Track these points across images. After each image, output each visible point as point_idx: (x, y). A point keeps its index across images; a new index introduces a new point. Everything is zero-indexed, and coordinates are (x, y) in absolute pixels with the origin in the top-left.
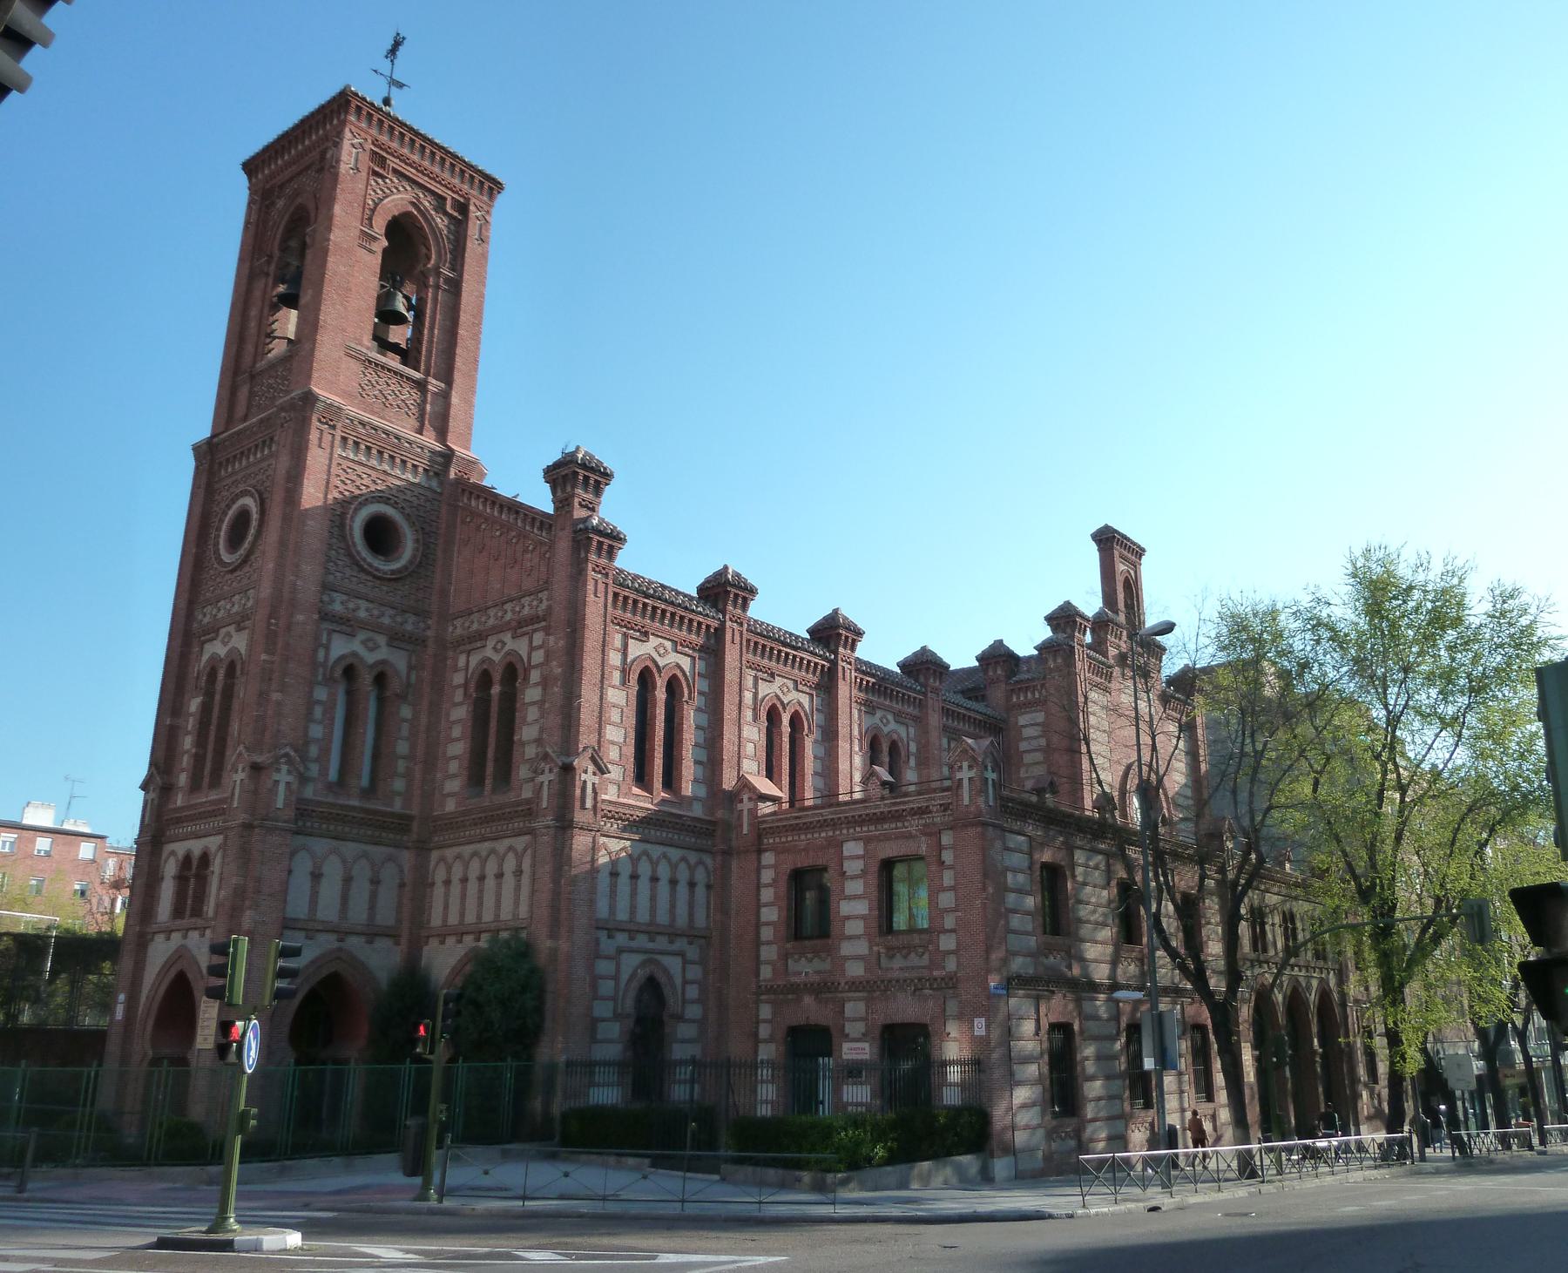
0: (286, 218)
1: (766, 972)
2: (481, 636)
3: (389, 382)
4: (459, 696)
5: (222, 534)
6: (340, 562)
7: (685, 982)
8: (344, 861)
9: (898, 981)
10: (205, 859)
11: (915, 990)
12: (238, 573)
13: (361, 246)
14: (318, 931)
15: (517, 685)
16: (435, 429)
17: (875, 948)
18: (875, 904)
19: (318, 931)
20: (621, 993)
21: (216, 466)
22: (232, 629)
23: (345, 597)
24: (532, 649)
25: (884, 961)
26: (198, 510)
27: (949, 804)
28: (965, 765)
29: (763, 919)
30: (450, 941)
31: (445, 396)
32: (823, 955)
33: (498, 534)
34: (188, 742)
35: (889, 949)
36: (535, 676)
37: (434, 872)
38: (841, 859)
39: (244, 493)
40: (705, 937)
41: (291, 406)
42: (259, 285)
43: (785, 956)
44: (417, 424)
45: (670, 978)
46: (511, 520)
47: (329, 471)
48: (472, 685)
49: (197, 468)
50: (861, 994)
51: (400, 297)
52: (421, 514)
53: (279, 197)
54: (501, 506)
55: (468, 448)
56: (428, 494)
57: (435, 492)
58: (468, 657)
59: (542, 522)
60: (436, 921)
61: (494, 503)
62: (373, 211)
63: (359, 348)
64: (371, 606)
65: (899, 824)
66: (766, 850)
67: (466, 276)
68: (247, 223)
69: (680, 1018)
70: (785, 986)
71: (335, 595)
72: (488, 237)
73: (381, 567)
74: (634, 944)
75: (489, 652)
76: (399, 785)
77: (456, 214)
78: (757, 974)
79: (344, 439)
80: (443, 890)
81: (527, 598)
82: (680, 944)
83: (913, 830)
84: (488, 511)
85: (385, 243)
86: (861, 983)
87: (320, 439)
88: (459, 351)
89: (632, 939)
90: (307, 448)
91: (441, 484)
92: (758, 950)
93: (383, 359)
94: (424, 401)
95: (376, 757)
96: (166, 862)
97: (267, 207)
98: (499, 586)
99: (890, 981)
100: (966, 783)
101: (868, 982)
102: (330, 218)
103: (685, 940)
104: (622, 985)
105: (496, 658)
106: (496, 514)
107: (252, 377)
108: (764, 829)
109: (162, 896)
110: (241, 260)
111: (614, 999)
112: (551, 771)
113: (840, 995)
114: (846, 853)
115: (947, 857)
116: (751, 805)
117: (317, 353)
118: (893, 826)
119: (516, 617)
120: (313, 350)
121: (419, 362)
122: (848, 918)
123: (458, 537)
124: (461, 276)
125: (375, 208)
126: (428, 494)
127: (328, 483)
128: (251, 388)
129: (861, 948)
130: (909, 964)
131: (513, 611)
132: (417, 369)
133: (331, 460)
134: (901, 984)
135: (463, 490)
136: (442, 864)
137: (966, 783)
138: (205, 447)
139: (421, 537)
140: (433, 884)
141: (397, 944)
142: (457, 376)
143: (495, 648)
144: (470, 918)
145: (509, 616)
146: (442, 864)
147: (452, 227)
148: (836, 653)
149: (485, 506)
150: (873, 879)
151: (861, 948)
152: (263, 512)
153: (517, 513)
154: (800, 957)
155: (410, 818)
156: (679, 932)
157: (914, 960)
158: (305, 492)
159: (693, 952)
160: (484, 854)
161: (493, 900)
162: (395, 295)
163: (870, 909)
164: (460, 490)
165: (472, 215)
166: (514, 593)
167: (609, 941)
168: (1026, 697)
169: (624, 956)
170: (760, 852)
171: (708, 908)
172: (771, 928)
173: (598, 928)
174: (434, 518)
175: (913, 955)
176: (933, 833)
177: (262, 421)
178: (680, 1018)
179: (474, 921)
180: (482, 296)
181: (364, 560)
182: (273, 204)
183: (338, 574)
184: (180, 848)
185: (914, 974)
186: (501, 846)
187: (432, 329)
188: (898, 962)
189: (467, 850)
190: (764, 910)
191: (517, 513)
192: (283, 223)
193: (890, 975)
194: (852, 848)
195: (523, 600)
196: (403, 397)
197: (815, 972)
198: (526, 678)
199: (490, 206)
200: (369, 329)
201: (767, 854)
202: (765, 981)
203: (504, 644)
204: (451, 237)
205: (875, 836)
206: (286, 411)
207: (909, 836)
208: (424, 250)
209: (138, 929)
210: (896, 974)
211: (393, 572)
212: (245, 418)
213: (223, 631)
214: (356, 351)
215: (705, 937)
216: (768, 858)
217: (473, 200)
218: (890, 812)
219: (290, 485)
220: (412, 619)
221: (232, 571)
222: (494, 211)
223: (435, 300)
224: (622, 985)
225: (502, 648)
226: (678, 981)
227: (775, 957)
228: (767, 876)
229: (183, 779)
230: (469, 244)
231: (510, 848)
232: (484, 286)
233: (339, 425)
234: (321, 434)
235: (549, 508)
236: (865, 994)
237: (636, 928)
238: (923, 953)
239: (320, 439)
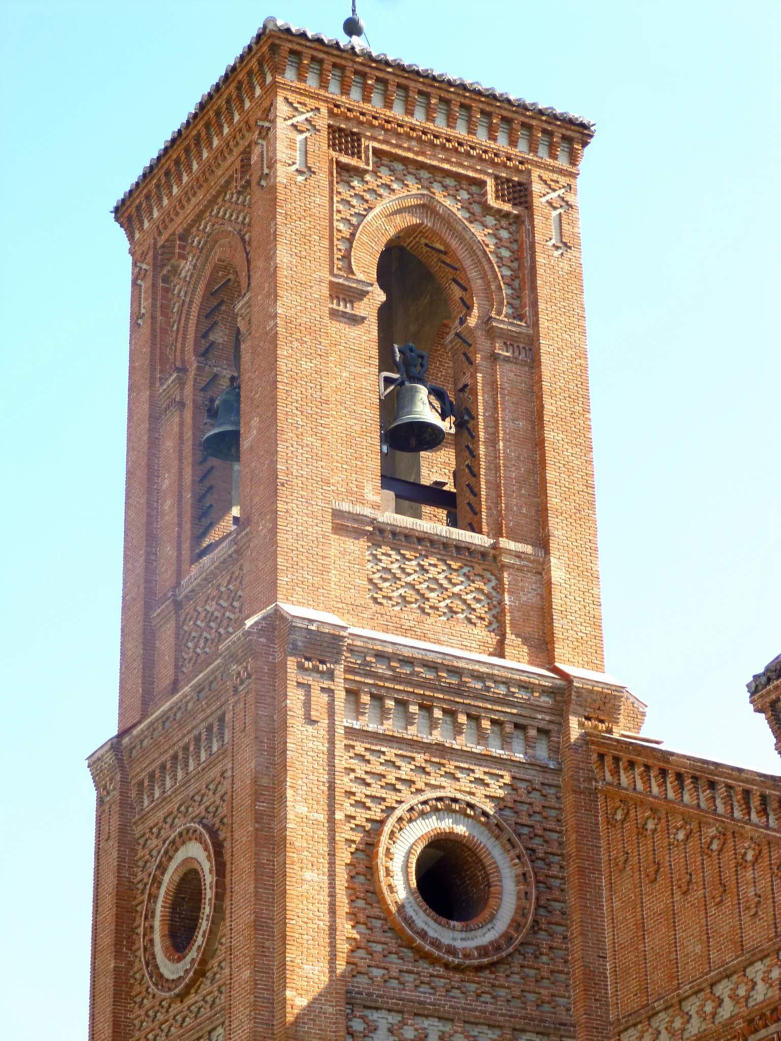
0: (200, 291)
3: (425, 563)
5: (157, 923)
6: (379, 948)
12: (192, 999)
13: (334, 314)
16: (525, 641)
23: (394, 1018)
26: (110, 881)
31: (541, 570)
33: (681, 836)
39: (184, 837)
41: (248, 649)
42: (172, 423)
44: (493, 639)
46: (703, 805)
47: (331, 765)
49: (101, 801)
51: (423, 392)
52: (525, 820)
53: (183, 257)
54: (679, 777)
55: (599, 668)
56: (530, 774)
57: (544, 769)
59: (764, 798)
61: (663, 773)
62: (350, 240)
63: (358, 509)
64: (448, 1028)
67: (544, 323)
68: (136, 318)
71: (374, 1016)
72: (576, 236)
73: (459, 944)
77: (507, 207)
79: (353, 693)
81: (759, 966)
84: (655, 790)
85: (380, 296)
87: (307, 704)
88: (551, 475)
90: (284, 727)
91: (555, 750)
93: (405, 521)
94: (499, 588)
97: (165, 279)
98: (698, 949)
102: (273, 275)
106: (671, 795)
107: (178, 605)
110: (132, 388)
117: (281, 537)
119: (744, 1011)
120: (273, 531)
121: (476, 512)
123: (604, 857)
124: (536, 324)
125: (353, 235)
126: (530, 774)
127: (332, 787)
128: (178, 627)
131: (734, 997)
132: (475, 527)
133: (332, 742)
135: (601, 756)
138: (110, 759)
139: (529, 868)
142: (558, 529)
147: (504, 234)
149: (647, 782)
152: (220, 869)
153: (712, 785)
158: (290, 816)
162: (413, 393)
164: (594, 757)
165: (539, 202)
166: (731, 958)
174: (552, 825)
177: (199, 689)
180: (582, 354)
181: (423, 935)
182: (175, 270)
183: (377, 972)
187: (493, 442)
191: (712, 785)
192: (197, 300)
195: (750, 971)
196: (456, 590)
199: (574, 175)
200: (374, 464)
204: (505, 253)
208: (457, 292)
211: (483, 951)
212: (175, 687)
214: (357, 518)
219: (262, 806)
221: (182, 997)
222: (580, 183)
223: (492, 385)
230: (540, 259)
232: (583, 333)
233: (339, 670)
234: (308, 695)
239: (307, 704)
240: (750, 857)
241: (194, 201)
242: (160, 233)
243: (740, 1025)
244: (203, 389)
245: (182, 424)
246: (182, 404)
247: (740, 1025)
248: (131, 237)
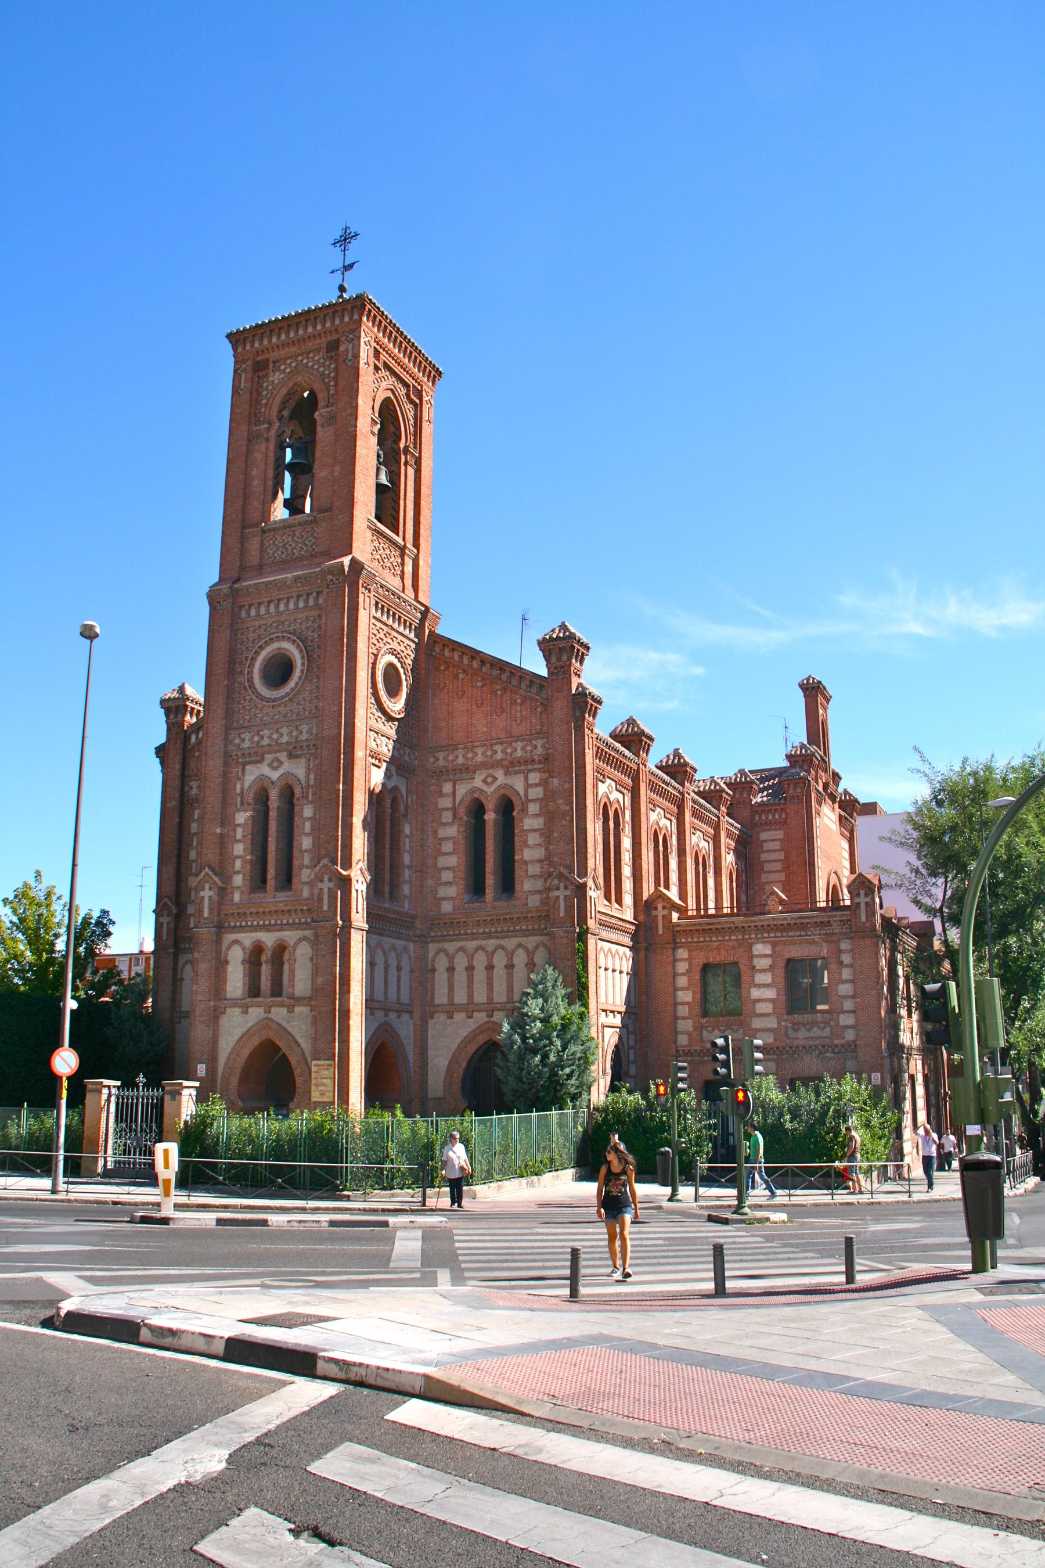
0: (284, 391)
1: (683, 1040)
2: (468, 770)
4: (447, 817)
8: (384, 953)
9: (804, 1047)
10: (281, 949)
11: (820, 1053)
12: (282, 708)
14: (376, 1009)
15: (515, 813)
17: (783, 1024)
18: (782, 992)
19: (376, 1009)
21: (236, 610)
22: (283, 756)
24: (528, 786)
25: (790, 1032)
27: (848, 920)
28: (862, 892)
30: (460, 1017)
32: (735, 1028)
33: (479, 684)
34: (239, 849)
35: (794, 1024)
36: (533, 808)
37: (433, 961)
38: (751, 957)
40: (635, 1014)
43: (699, 1028)
48: (462, 811)
50: (771, 1057)
58: (454, 786)
59: (531, 681)
60: (441, 996)
65: (803, 933)
66: (680, 947)
70: (701, 1050)
75: (478, 782)
76: (406, 890)
78: (675, 1042)
80: (445, 976)
83: (816, 938)
86: (771, 1048)
95: (392, 866)
96: (229, 948)
99: (797, 1047)
100: (863, 906)
101: (778, 1048)
105: (490, 790)
108: (678, 931)
109: (228, 977)
112: (566, 888)
114: (755, 952)
115: (846, 959)
116: (665, 912)
118: (798, 934)
122: (759, 1000)
128: (262, 541)
129: (772, 1023)
130: (811, 1034)
134: (808, 1049)
136: (442, 954)
137: (863, 906)
140: (433, 970)
141: (411, 1018)
143: (484, 781)
144: (480, 997)
145: (499, 756)
146: (442, 954)
148: (683, 786)
150: (780, 973)
151: (772, 1023)
154: (714, 1029)
155: (414, 917)
157: (816, 1032)
160: (490, 949)
161: (505, 986)
163: (778, 995)
168: (767, 818)
170: (674, 949)
172: (686, 1007)
175: (815, 1029)
176: (832, 939)
179: (485, 1001)
184: (248, 939)
185: (818, 1042)
186: (510, 943)
188: (802, 1034)
189: (471, 945)
190: (679, 993)
193: (796, 1043)
194: (759, 948)
198: (524, 810)
201: (680, 950)
203: (495, 779)
205: (782, 941)
206: (333, 575)
207: (814, 942)
209: (212, 1003)
210: (803, 1042)
213: (269, 757)
216: (682, 953)
217: (424, 387)
218: (795, 924)
220: (408, 750)
225: (493, 782)
227: (691, 1029)
228: (682, 967)
229: (238, 880)
231: (520, 945)
233: (372, 588)
235: (543, 672)
236: (775, 1057)
238: (825, 1028)
240: (519, 701)
241: (286, 349)
242: (258, 355)
243: (506, 763)
244: (279, 436)
245: (267, 448)
246: (268, 440)
247: (506, 763)
248: (235, 349)
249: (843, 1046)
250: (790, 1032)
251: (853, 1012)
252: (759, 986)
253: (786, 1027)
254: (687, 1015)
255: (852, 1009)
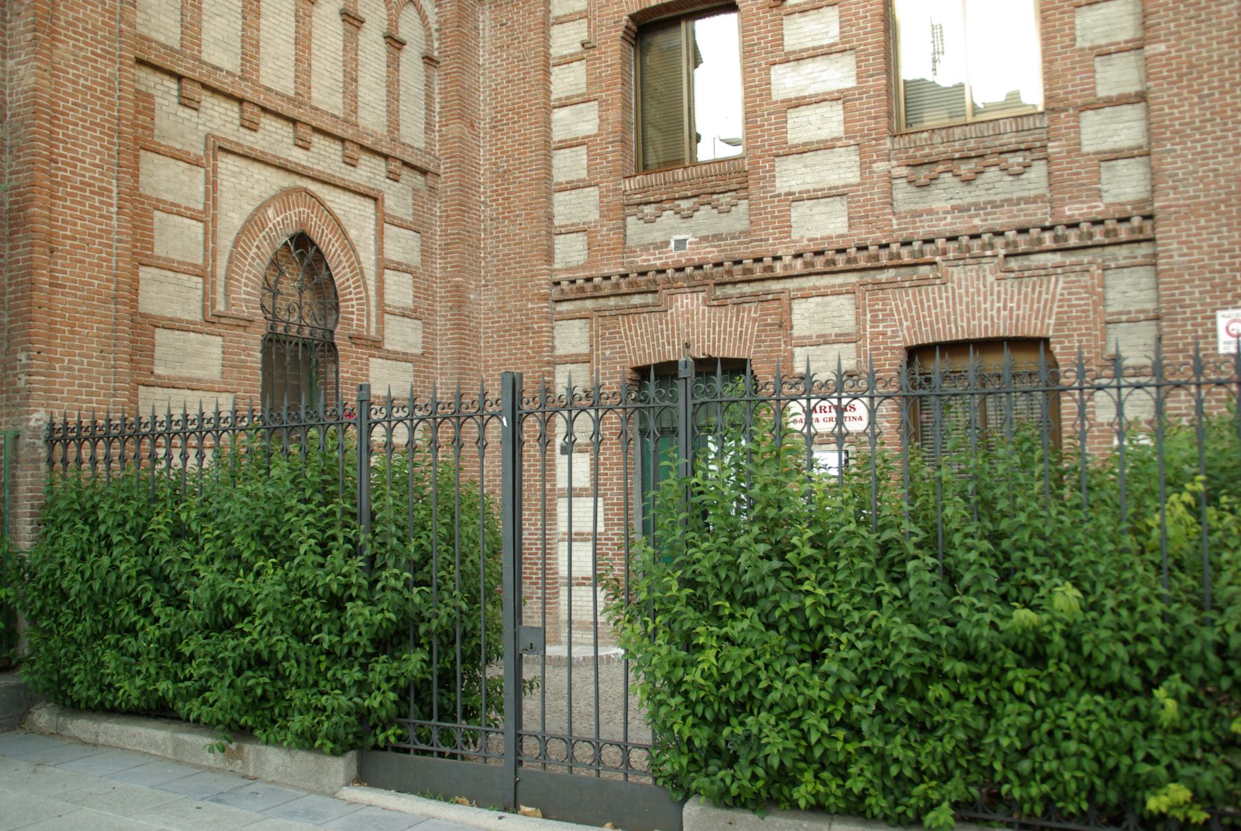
7: (383, 265)
17: (880, 167)
20: (222, 261)
29: (558, 135)
32: (726, 199)
40: (424, 172)
45: (350, 247)
69: (375, 345)
74: (248, 139)
78: (549, 256)
82: (369, 172)
89: (252, 127)
92: (549, 203)
103: (380, 164)
104: (225, 242)
111: (203, 273)
113: (776, 286)
122: (798, 103)
130: (974, 195)
156: (368, 142)
159: (398, 200)
167: (186, 113)
169: (227, 164)
171: (429, 108)
173: (140, 62)
175: (992, 174)
178: (375, 345)
185: (999, 220)
193: (923, 229)
197: (704, 239)
202: (567, 270)
210: (948, 224)
215: (424, 172)
224: (225, 242)
226: (368, 259)
227: (595, 216)
237: (262, 99)
249: (1096, 223)
250: (902, 192)
251: (1141, 97)
252: (798, 57)
253: (891, 179)
254: (583, 174)
255: (1133, 89)
